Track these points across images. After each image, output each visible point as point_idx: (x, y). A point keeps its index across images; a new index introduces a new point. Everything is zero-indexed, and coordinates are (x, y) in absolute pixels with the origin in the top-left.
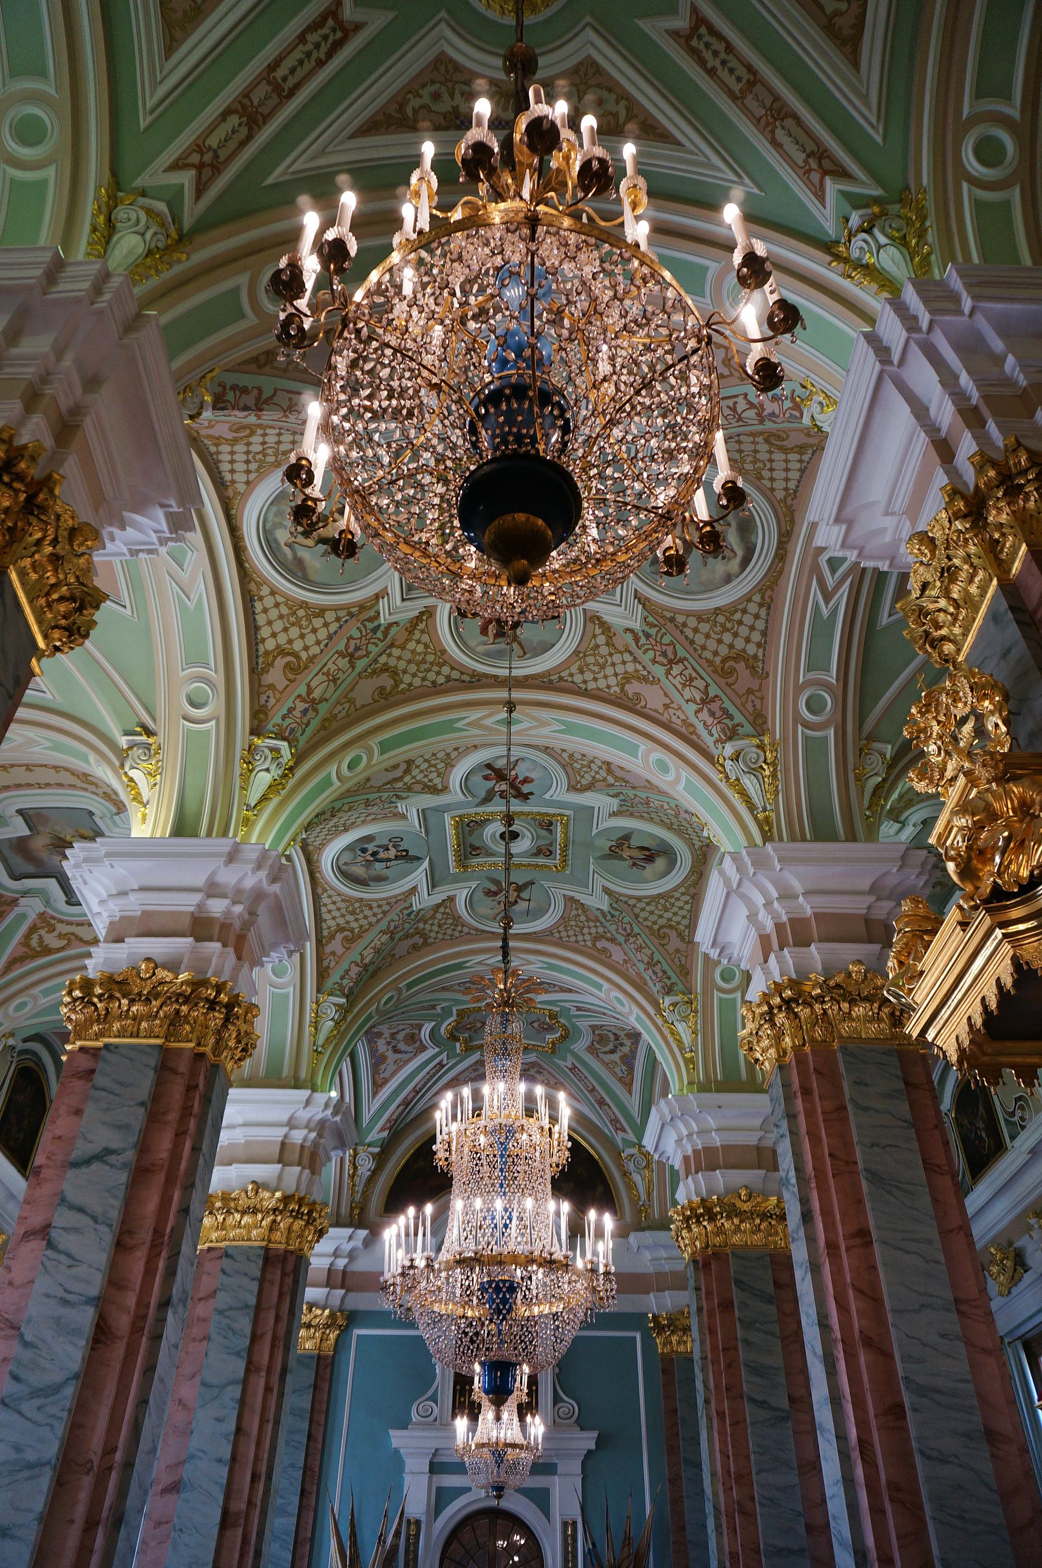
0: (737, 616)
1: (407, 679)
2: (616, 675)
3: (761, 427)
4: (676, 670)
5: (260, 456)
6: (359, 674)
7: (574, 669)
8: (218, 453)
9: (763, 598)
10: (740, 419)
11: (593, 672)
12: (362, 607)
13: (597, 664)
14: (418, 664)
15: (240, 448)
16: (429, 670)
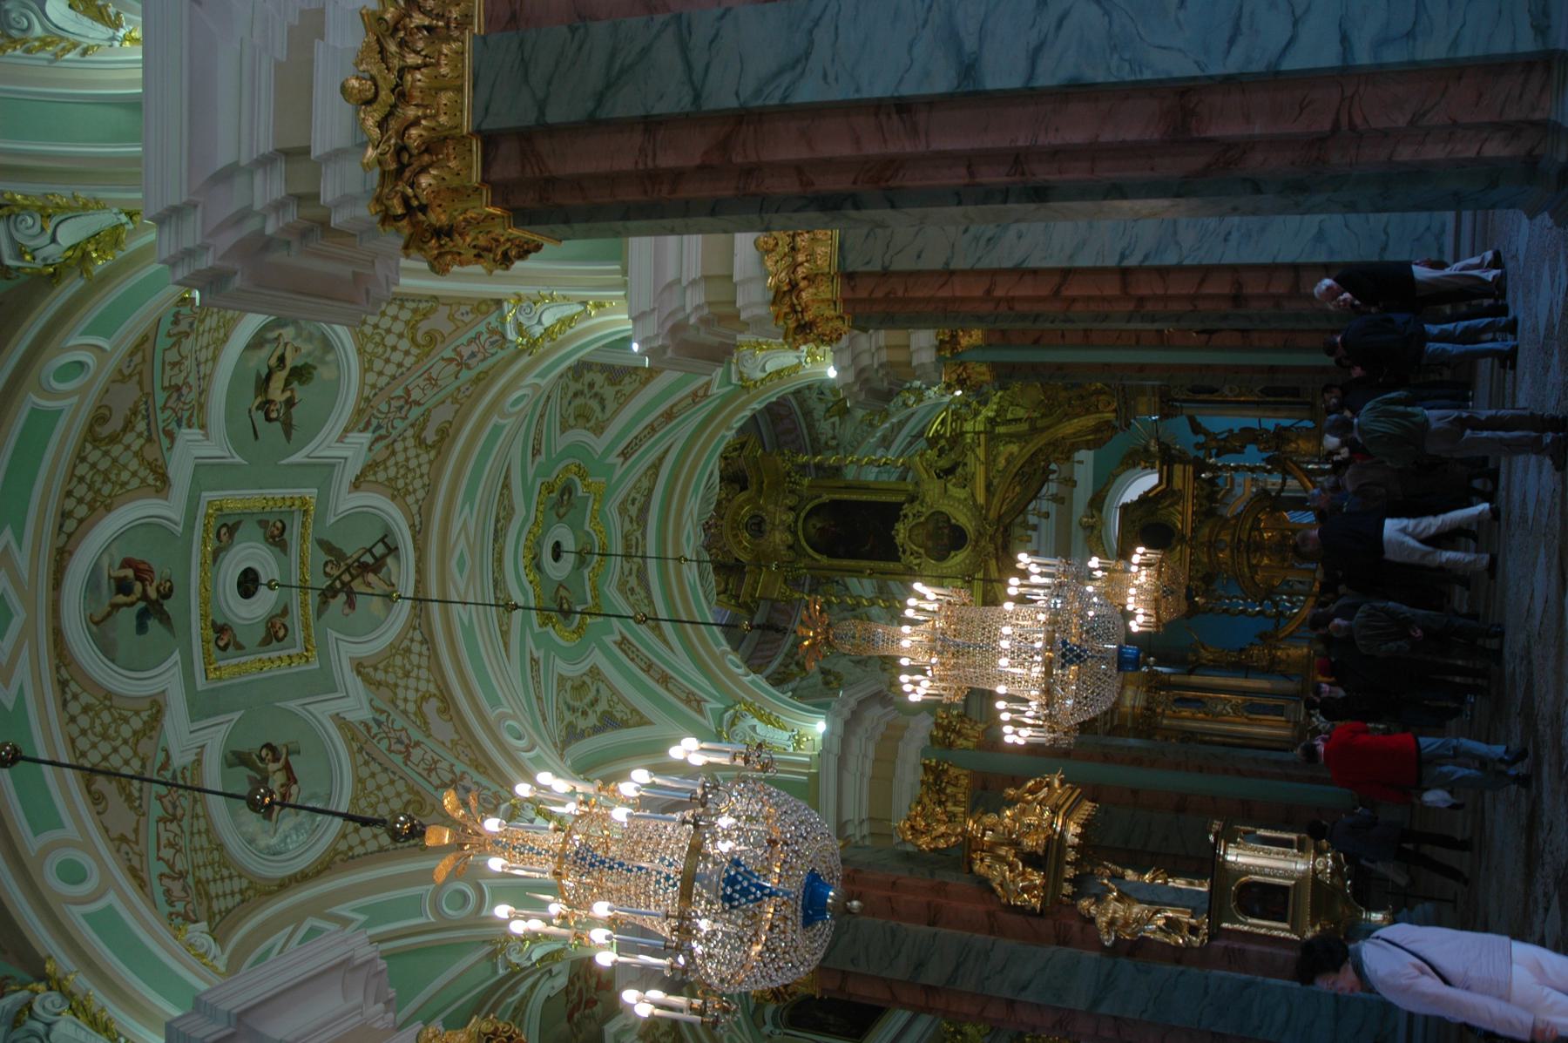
0: (225, 873)
1: (94, 456)
2: (105, 758)
3: (432, 790)
4: (173, 827)
5: (378, 339)
6: (149, 396)
7: (85, 698)
8: (402, 307)
9: (247, 889)
10: (430, 770)
11: (92, 727)
12: (201, 406)
13: (106, 728)
14: (106, 473)
15: (398, 327)
16: (90, 488)
